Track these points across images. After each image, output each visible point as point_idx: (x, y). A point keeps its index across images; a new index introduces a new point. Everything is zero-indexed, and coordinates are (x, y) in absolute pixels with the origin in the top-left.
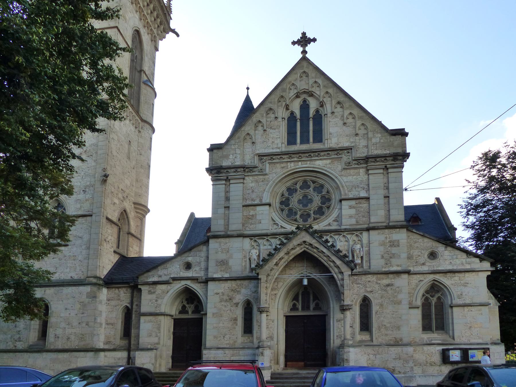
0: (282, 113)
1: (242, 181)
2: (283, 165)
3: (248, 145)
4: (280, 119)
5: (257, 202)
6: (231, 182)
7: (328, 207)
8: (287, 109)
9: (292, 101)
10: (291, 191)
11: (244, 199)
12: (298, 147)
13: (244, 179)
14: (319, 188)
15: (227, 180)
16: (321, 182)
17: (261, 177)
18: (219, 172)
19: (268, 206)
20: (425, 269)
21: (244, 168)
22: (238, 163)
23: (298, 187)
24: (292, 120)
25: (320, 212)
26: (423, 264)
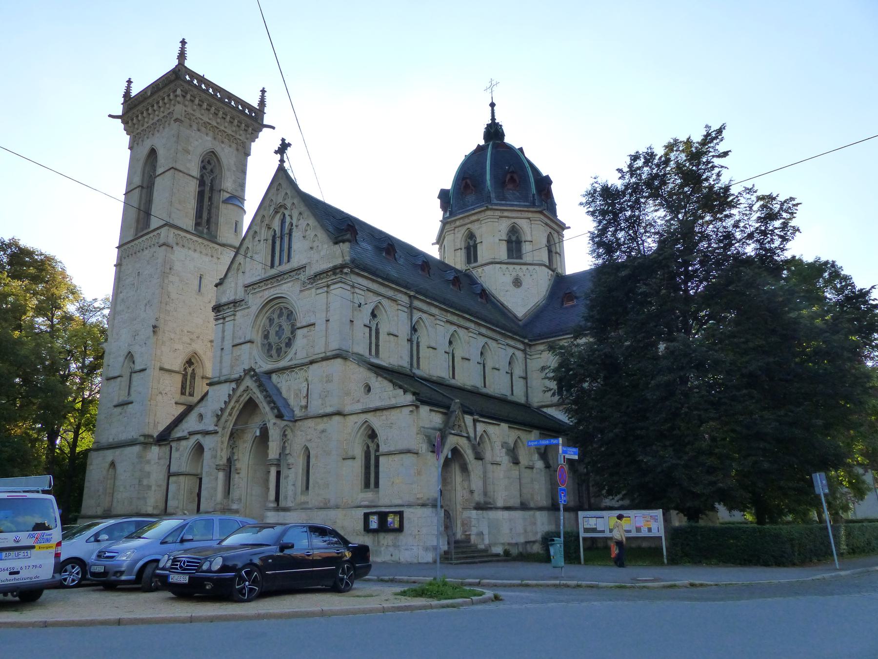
0: (264, 234)
1: (232, 318)
2: (261, 294)
3: (240, 274)
4: (262, 242)
5: (242, 340)
6: (227, 319)
7: (294, 337)
8: (269, 228)
9: (273, 217)
10: (271, 320)
11: (233, 338)
12: (273, 272)
13: (234, 315)
14: (290, 315)
15: (224, 318)
16: (291, 308)
17: (247, 311)
18: (219, 311)
19: (249, 345)
20: (359, 407)
21: (235, 303)
22: (232, 298)
23: (275, 316)
24: (274, 237)
25: (289, 344)
26: (358, 401)
